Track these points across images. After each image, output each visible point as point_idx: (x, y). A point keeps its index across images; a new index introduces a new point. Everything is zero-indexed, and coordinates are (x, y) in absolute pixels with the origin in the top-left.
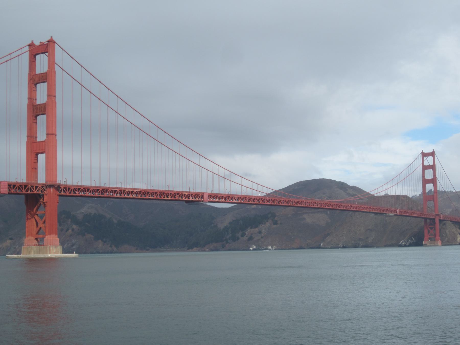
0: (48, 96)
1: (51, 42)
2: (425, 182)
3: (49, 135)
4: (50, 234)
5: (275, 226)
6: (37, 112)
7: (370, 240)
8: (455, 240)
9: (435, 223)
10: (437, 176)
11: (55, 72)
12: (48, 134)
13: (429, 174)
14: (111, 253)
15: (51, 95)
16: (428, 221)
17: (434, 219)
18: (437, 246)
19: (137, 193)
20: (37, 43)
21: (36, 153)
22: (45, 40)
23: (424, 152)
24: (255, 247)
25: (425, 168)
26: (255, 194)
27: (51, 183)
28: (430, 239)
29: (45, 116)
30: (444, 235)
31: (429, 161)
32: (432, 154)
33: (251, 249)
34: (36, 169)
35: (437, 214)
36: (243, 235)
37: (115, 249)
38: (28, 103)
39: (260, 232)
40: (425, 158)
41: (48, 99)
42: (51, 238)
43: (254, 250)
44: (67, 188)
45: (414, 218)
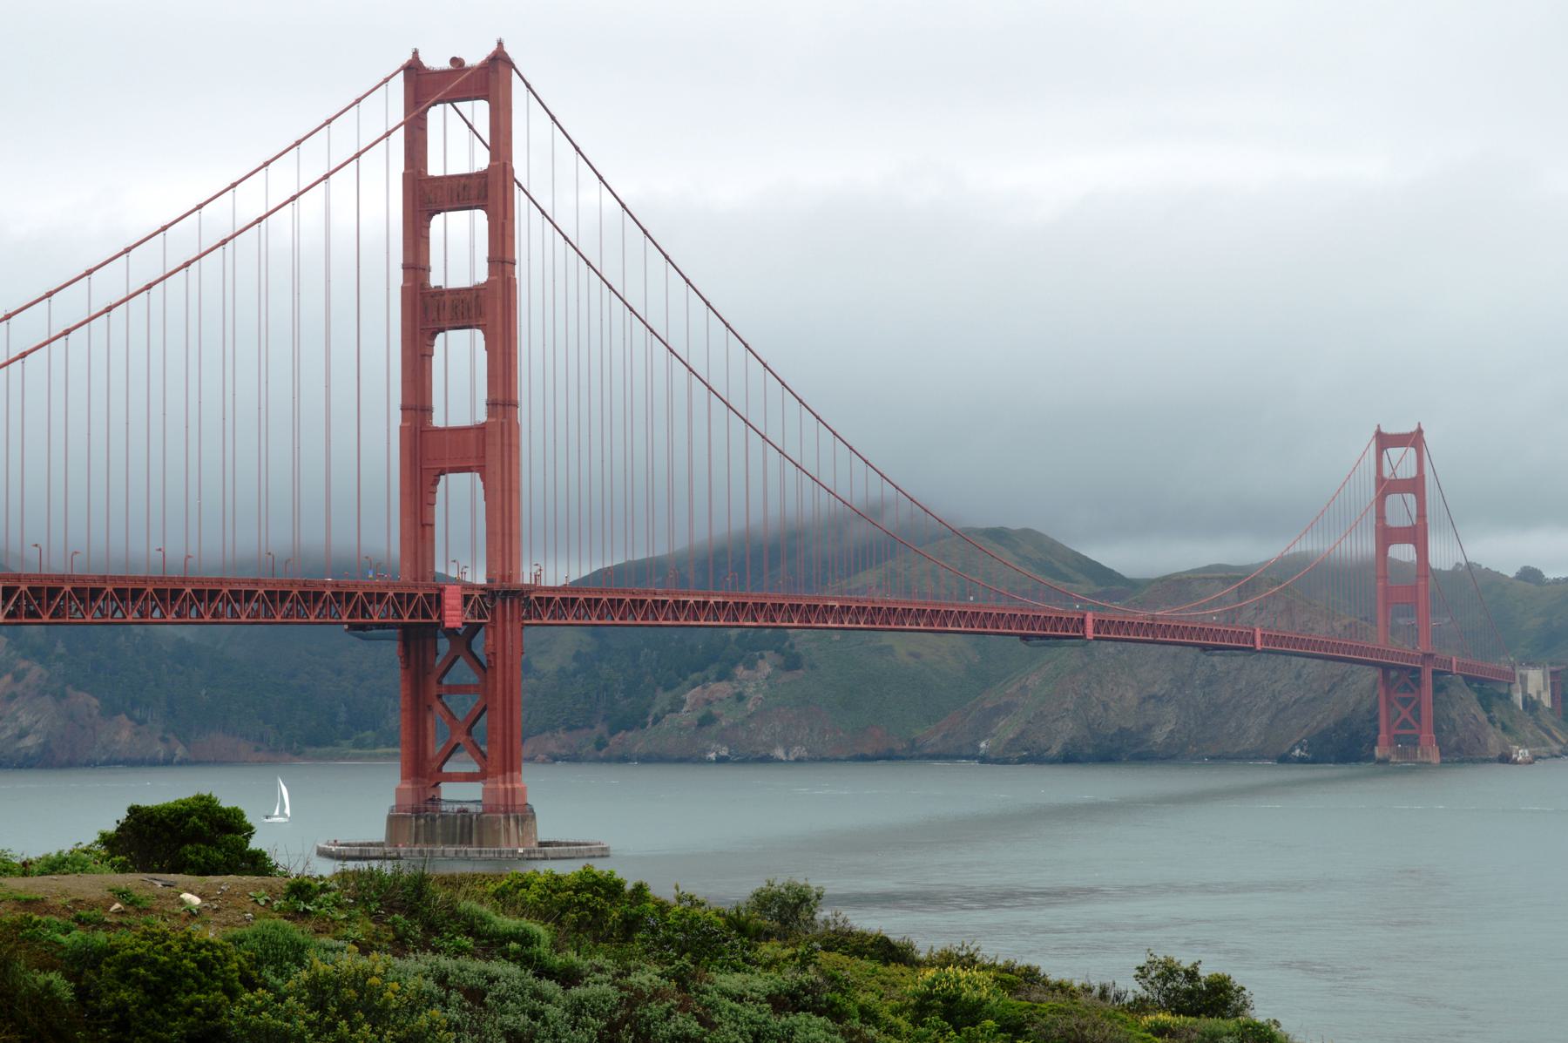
2: (1387, 536)
3: (500, 408)
6: (441, 318)
7: (1159, 735)
8: (1479, 741)
9: (1418, 683)
12: (492, 404)
13: (1400, 510)
17: (1417, 671)
18: (1425, 766)
20: (436, 60)
21: (437, 472)
23: (1383, 430)
25: (1386, 487)
30: (1445, 727)
32: (1415, 440)
35: (1426, 652)
38: (404, 282)
41: (491, 273)
42: (509, 786)
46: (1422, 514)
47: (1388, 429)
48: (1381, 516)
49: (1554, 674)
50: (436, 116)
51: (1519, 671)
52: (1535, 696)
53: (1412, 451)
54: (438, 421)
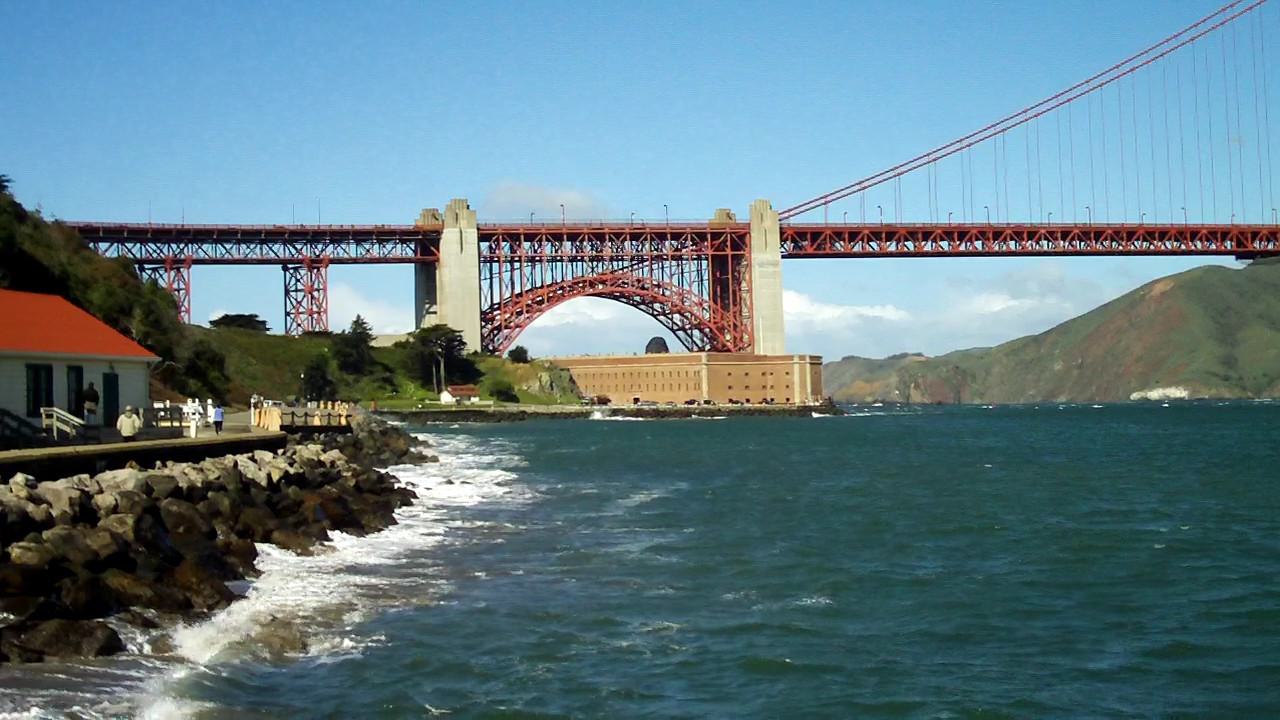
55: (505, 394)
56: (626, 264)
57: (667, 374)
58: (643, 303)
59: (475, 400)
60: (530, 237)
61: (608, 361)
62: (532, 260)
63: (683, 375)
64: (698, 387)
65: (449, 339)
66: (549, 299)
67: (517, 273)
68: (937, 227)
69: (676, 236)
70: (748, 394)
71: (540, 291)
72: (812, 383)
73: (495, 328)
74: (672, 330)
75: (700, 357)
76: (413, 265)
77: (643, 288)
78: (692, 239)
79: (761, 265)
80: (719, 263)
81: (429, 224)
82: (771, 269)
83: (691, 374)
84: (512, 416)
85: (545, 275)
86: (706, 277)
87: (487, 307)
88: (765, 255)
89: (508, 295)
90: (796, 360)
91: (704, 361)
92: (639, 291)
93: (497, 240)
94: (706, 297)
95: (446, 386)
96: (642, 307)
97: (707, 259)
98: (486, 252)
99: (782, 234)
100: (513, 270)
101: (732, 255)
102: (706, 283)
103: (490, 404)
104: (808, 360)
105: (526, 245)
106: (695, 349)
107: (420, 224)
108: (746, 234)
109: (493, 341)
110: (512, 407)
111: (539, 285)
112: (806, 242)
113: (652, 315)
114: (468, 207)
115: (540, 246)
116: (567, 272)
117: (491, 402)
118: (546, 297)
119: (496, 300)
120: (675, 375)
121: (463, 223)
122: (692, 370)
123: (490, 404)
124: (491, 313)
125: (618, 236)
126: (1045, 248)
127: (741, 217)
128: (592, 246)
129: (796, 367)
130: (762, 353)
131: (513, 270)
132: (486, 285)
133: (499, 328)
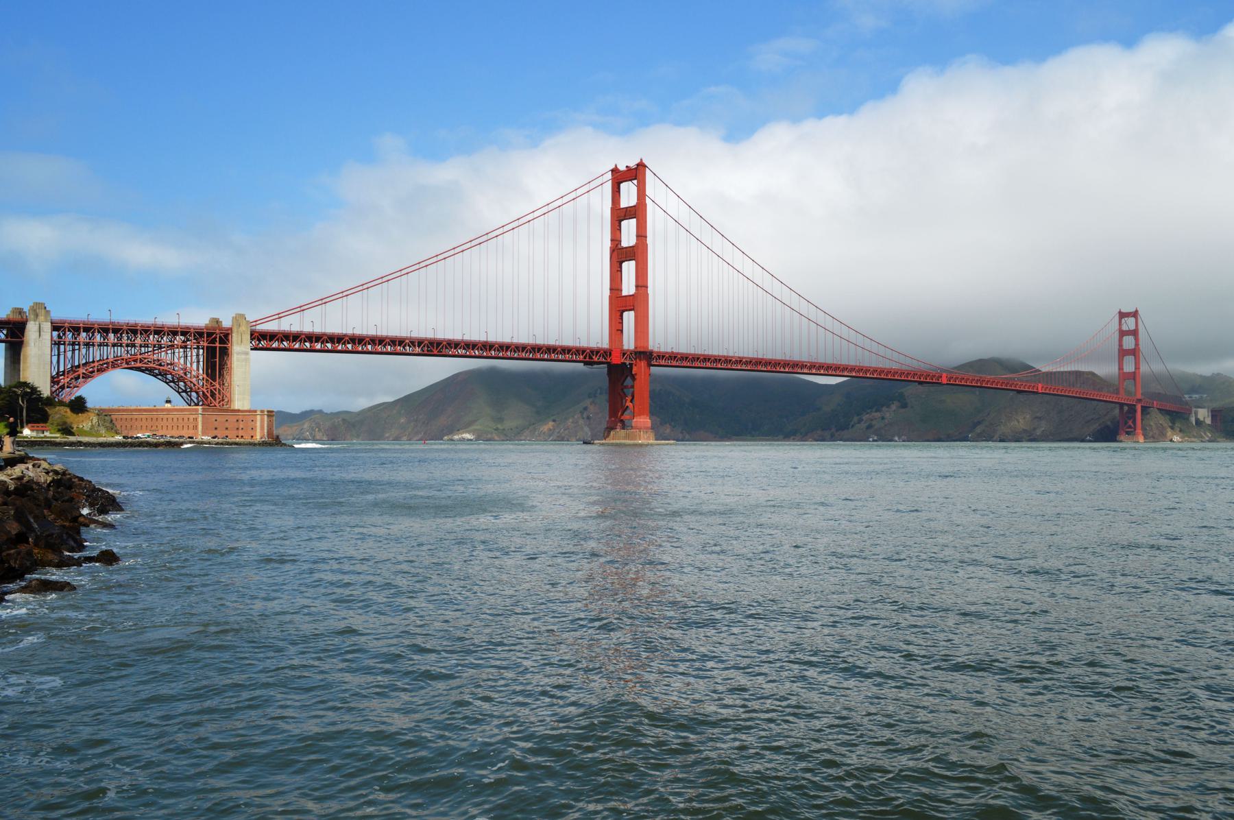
0: (638, 236)
1: (641, 166)
4: (640, 414)
5: (903, 410)
7: (1038, 432)
9: (1135, 411)
10: (1141, 346)
11: (646, 205)
12: (637, 287)
13: (1129, 342)
14: (683, 441)
15: (641, 235)
16: (1126, 408)
19: (746, 363)
20: (622, 168)
22: (632, 164)
23: (1122, 311)
24: (875, 438)
25: (1122, 333)
26: (895, 366)
27: (642, 350)
28: (1128, 433)
29: (633, 263)
31: (1130, 324)
32: (1135, 314)
33: (871, 439)
34: (622, 331)
36: (860, 421)
37: (687, 437)
39: (883, 418)
40: (1123, 320)
43: (874, 441)
44: (661, 356)
45: (1103, 403)
46: (1137, 344)
47: (1124, 310)
48: (1121, 345)
49: (1212, 411)
50: (624, 186)
51: (1194, 409)
52: (1202, 419)
53: (1133, 319)
54: (625, 293)
55: (67, 430)
56: (150, 349)
57: (175, 420)
58: (160, 374)
59: (47, 434)
60: (87, 330)
61: (136, 410)
62: (87, 345)
63: (186, 420)
64: (196, 427)
65: (32, 393)
66: (98, 370)
67: (77, 352)
68: (346, 335)
69: (184, 333)
70: (227, 433)
71: (92, 365)
72: (268, 426)
73: (60, 387)
74: (178, 392)
75: (197, 410)
76: (4, 344)
77: (160, 365)
78: (195, 336)
79: (238, 353)
80: (211, 352)
81: (17, 318)
82: (243, 356)
83: (191, 420)
84: (71, 444)
85: (96, 354)
86: (201, 360)
87: (54, 373)
88: (240, 348)
89: (69, 366)
90: (258, 413)
91: (200, 412)
92: (158, 367)
93: (64, 331)
94: (201, 371)
95: (27, 424)
96: (159, 377)
97: (203, 349)
98: (55, 338)
99: (252, 335)
100: (74, 350)
101: (220, 347)
102: (201, 363)
103: (58, 437)
104: (266, 413)
105: (84, 335)
106: (192, 404)
107: (11, 317)
108: (228, 334)
109: (58, 395)
110: (72, 439)
111: (91, 360)
112: (264, 339)
113: (166, 382)
114: (45, 308)
115: (93, 335)
116: (110, 353)
117: (58, 435)
118: (96, 369)
119: (62, 369)
120: (180, 421)
121: (41, 318)
122: (192, 417)
123: (58, 437)
124: (58, 377)
125: (146, 331)
126: (389, 350)
127: (226, 323)
128: (128, 337)
129: (258, 417)
130: (236, 408)
131: (74, 350)
132: (55, 359)
133: (63, 388)
